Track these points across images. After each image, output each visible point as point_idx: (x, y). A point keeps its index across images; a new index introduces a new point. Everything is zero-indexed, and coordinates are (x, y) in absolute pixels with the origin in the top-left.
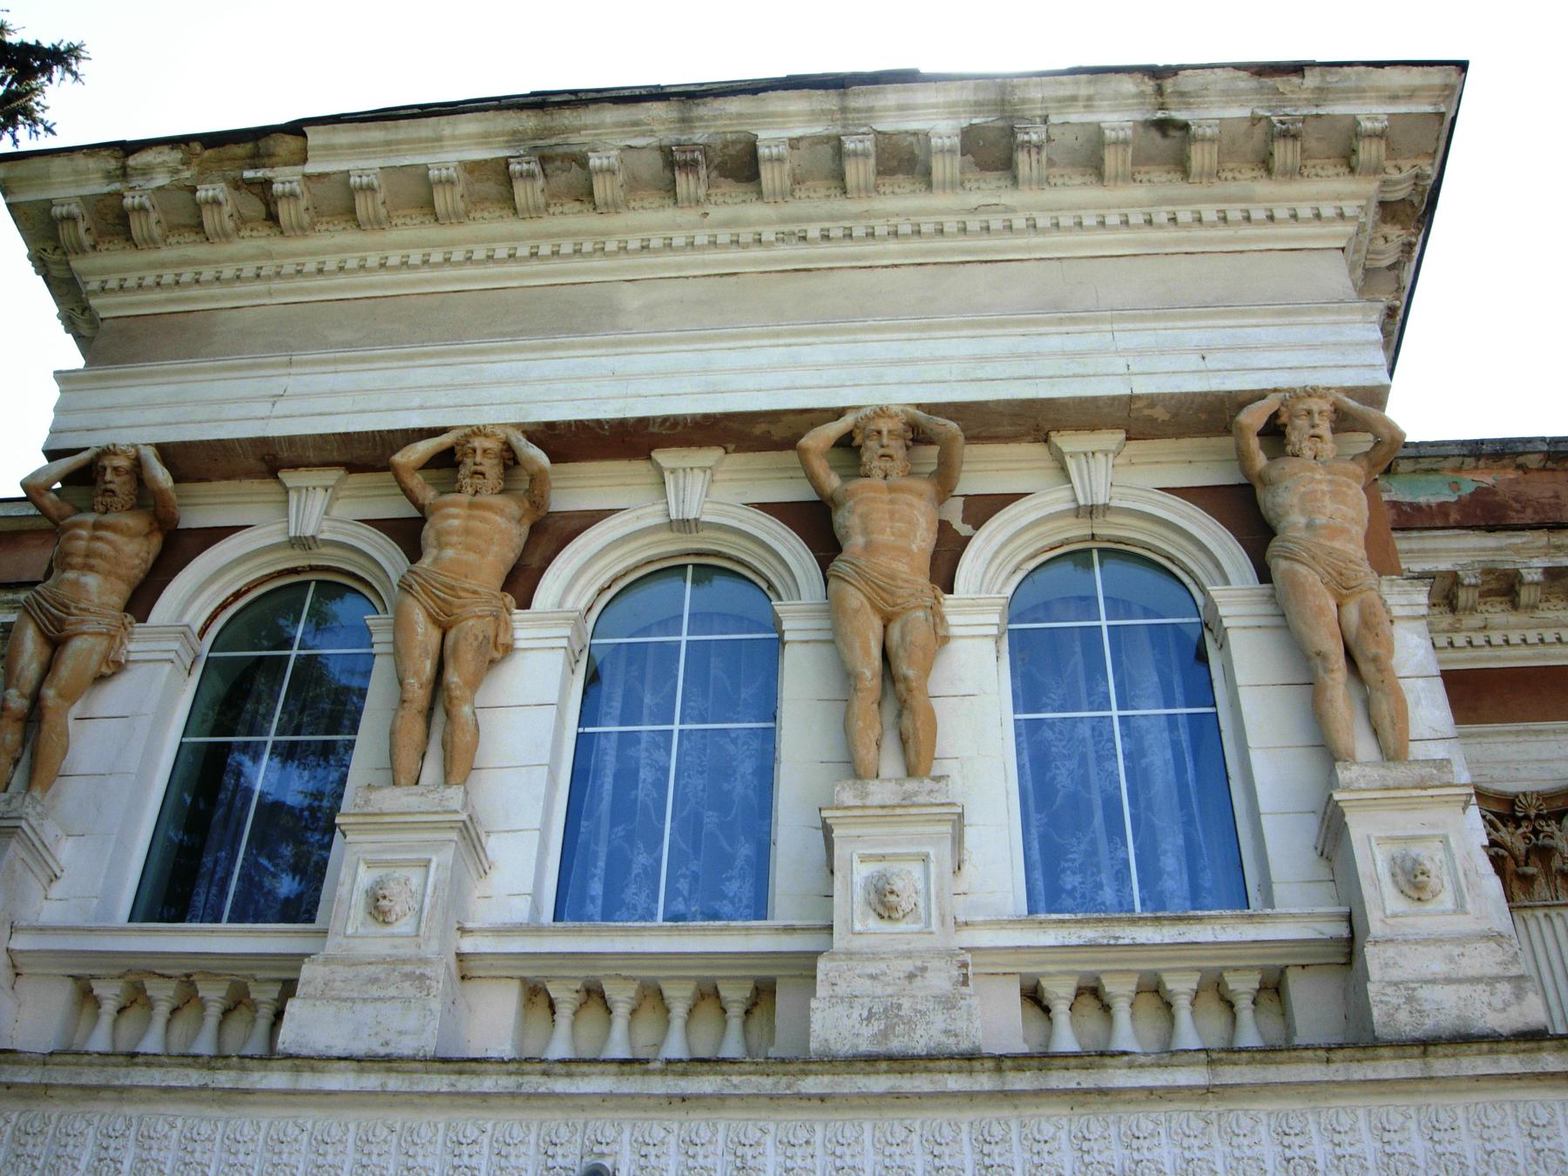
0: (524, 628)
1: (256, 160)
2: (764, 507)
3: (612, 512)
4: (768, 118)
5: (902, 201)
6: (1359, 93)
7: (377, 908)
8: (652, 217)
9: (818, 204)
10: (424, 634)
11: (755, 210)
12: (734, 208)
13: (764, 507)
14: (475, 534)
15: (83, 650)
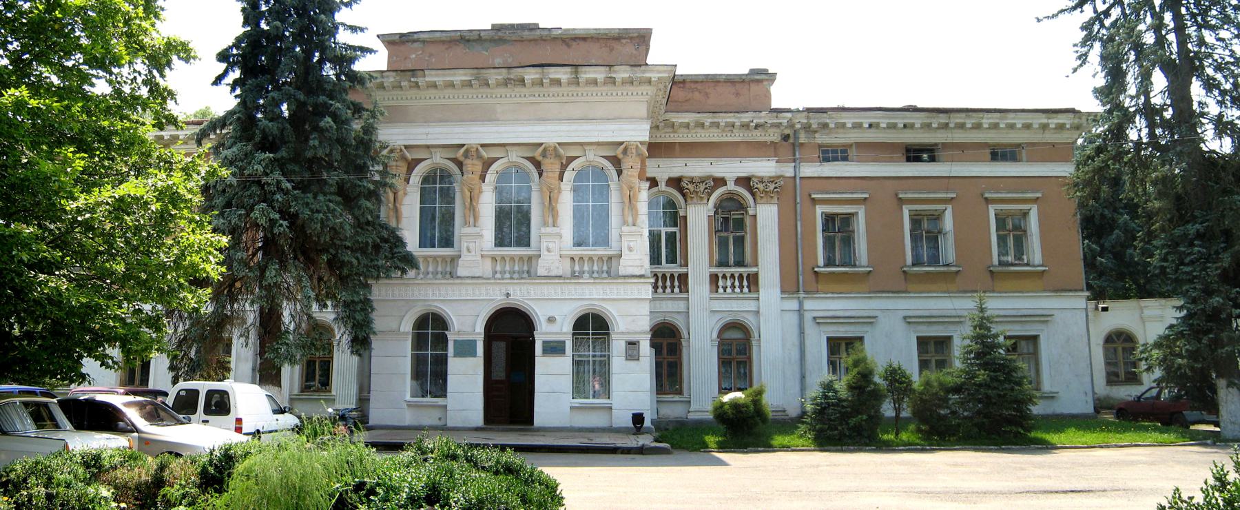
0: (484, 187)
1: (413, 76)
2: (527, 158)
3: (497, 159)
4: (529, 73)
5: (555, 89)
6: (652, 71)
7: (468, 250)
8: (502, 91)
9: (537, 89)
10: (468, 194)
11: (524, 90)
12: (519, 90)
13: (527, 158)
14: (473, 166)
15: (400, 193)
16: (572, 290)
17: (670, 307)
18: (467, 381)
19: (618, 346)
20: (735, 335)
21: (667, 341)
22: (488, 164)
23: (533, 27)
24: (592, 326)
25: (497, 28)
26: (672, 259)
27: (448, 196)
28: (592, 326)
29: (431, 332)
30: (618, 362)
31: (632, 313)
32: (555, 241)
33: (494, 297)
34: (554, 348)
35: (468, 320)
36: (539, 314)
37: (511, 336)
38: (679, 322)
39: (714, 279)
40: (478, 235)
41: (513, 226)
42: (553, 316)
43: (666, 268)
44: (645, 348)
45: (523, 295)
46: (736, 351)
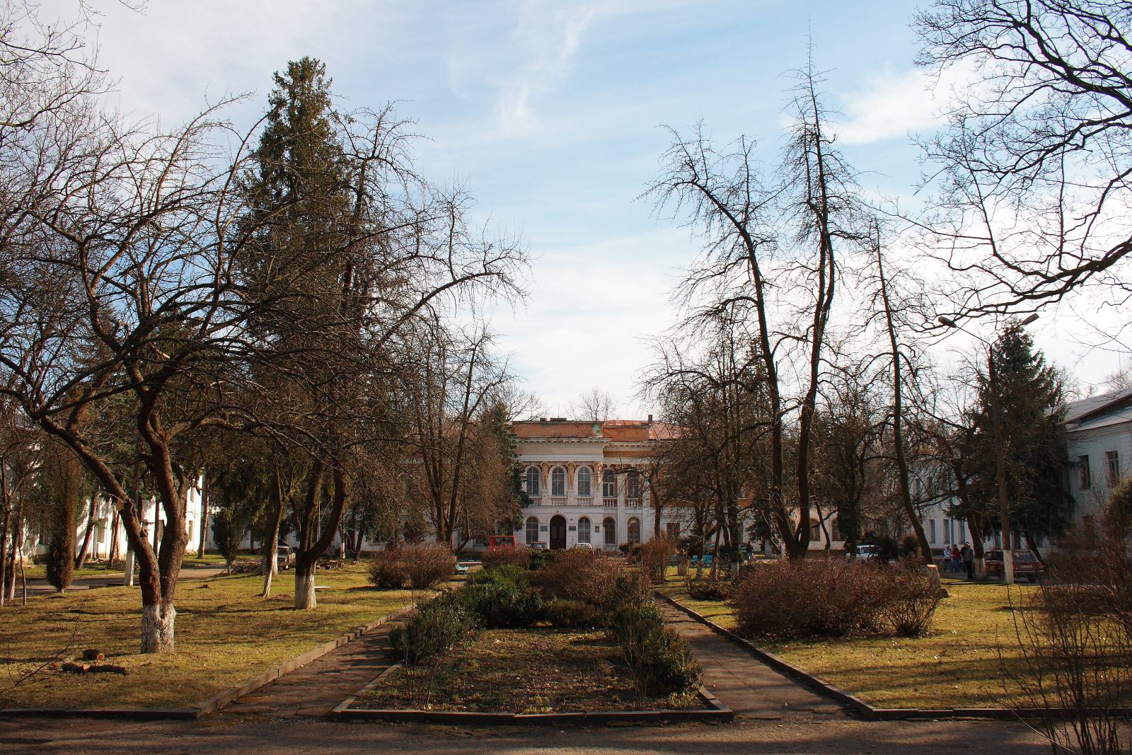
14: (545, 468)
16: (578, 510)
17: (610, 512)
18: (544, 537)
19: (592, 528)
20: (633, 522)
21: (609, 523)
22: (550, 468)
23: (564, 420)
24: (584, 521)
25: (553, 420)
26: (612, 494)
27: (536, 477)
28: (584, 521)
29: (533, 521)
30: (593, 533)
31: (597, 517)
32: (573, 492)
33: (553, 512)
34: (572, 529)
35: (545, 517)
36: (568, 517)
37: (558, 523)
38: (614, 518)
39: (626, 502)
40: (547, 490)
41: (558, 489)
42: (572, 517)
43: (610, 498)
44: (602, 529)
45: (562, 512)
46: (634, 528)
